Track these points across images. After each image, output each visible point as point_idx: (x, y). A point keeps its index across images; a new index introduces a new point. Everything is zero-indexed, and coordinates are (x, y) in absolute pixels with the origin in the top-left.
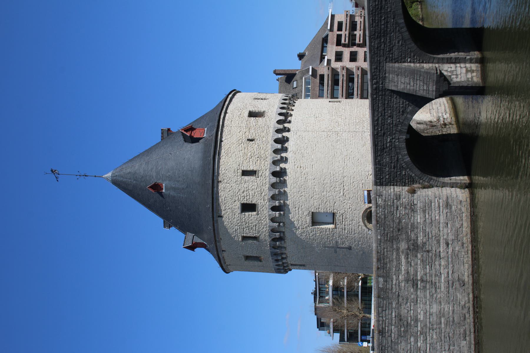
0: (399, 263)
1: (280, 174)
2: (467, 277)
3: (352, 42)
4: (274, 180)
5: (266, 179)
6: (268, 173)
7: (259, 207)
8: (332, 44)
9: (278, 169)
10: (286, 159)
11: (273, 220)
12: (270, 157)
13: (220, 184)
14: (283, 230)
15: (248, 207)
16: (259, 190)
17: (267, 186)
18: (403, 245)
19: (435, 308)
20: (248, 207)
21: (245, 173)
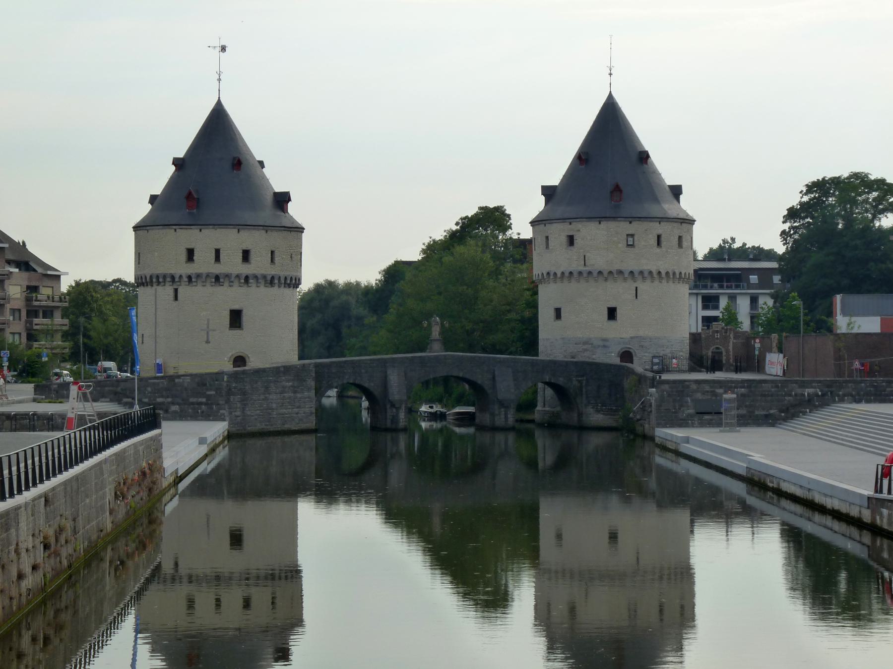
0: (288, 381)
1: (271, 281)
2: (287, 427)
3: (32, 313)
4: (269, 278)
5: (271, 271)
6: (273, 273)
7: (246, 265)
8: (29, 279)
9: (276, 281)
10: (279, 287)
11: (238, 276)
12: (283, 274)
13: (264, 232)
14: (226, 284)
15: (246, 256)
16: (259, 265)
17: (265, 273)
18: (296, 384)
19: (274, 406)
20: (246, 256)
21: (272, 252)
